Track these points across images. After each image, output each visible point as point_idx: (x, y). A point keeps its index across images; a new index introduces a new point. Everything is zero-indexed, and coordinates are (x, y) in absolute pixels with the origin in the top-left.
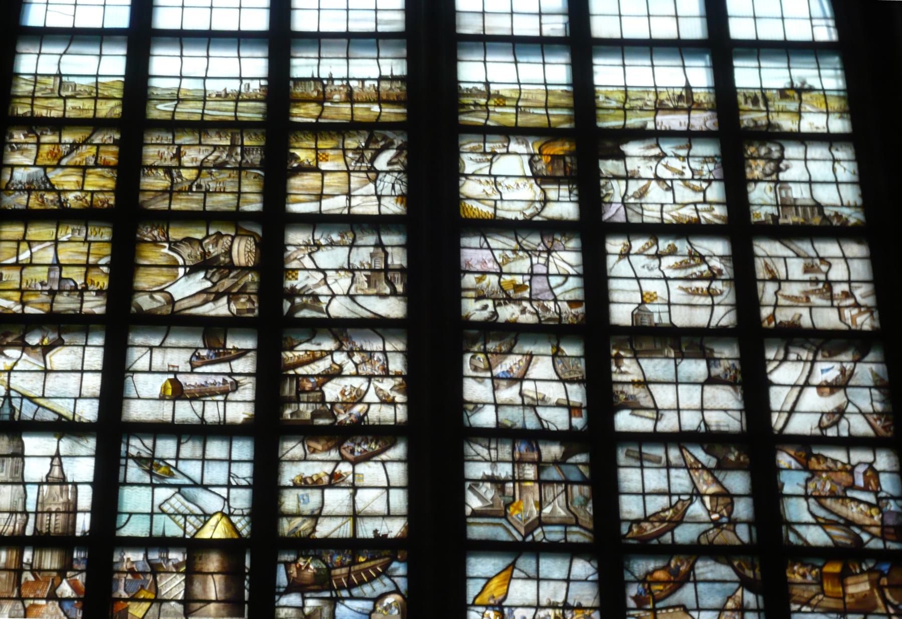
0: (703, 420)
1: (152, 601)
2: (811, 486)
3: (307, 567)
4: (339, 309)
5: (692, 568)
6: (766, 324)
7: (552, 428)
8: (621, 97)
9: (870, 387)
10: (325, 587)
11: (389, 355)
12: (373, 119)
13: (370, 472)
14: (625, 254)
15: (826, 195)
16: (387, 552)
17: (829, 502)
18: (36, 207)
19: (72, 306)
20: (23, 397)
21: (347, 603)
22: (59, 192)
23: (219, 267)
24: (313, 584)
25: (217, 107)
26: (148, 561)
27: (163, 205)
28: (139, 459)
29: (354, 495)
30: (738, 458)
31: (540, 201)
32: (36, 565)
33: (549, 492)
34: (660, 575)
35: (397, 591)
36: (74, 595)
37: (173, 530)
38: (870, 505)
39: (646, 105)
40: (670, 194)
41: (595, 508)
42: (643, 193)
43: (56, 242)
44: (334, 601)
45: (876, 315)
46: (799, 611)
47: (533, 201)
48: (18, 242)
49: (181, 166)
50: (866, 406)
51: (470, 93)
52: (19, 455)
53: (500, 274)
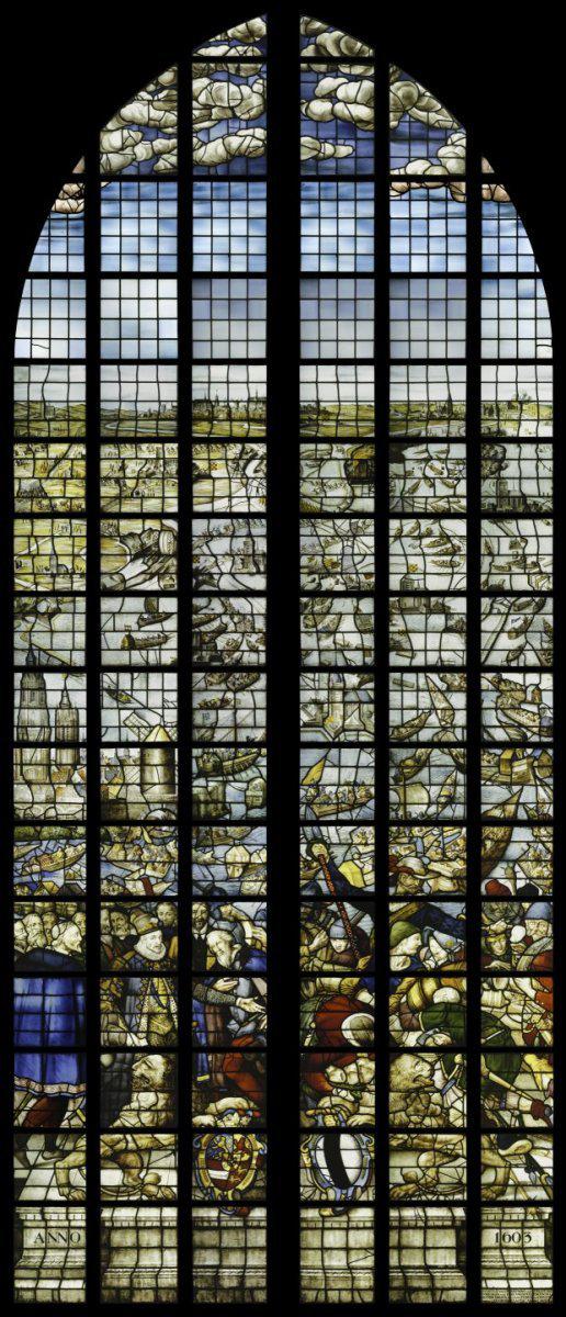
0: (440, 658)
1: (123, 785)
2: (500, 701)
4: (226, 583)
7: (353, 664)
8: (404, 409)
14: (399, 536)
15: (530, 488)
16: (255, 750)
17: (509, 712)
19: (66, 586)
20: (40, 649)
22: (51, 498)
26: (118, 758)
27: (114, 509)
28: (109, 691)
29: (235, 713)
33: (350, 708)
34: (409, 762)
35: (262, 777)
37: (133, 737)
38: (534, 714)
41: (376, 719)
43: (53, 537)
44: (225, 783)
45: (551, 579)
46: (485, 785)
47: (346, 498)
48: (29, 537)
49: (125, 477)
50: (537, 645)
51: (308, 410)
52: (43, 688)
53: (323, 556)
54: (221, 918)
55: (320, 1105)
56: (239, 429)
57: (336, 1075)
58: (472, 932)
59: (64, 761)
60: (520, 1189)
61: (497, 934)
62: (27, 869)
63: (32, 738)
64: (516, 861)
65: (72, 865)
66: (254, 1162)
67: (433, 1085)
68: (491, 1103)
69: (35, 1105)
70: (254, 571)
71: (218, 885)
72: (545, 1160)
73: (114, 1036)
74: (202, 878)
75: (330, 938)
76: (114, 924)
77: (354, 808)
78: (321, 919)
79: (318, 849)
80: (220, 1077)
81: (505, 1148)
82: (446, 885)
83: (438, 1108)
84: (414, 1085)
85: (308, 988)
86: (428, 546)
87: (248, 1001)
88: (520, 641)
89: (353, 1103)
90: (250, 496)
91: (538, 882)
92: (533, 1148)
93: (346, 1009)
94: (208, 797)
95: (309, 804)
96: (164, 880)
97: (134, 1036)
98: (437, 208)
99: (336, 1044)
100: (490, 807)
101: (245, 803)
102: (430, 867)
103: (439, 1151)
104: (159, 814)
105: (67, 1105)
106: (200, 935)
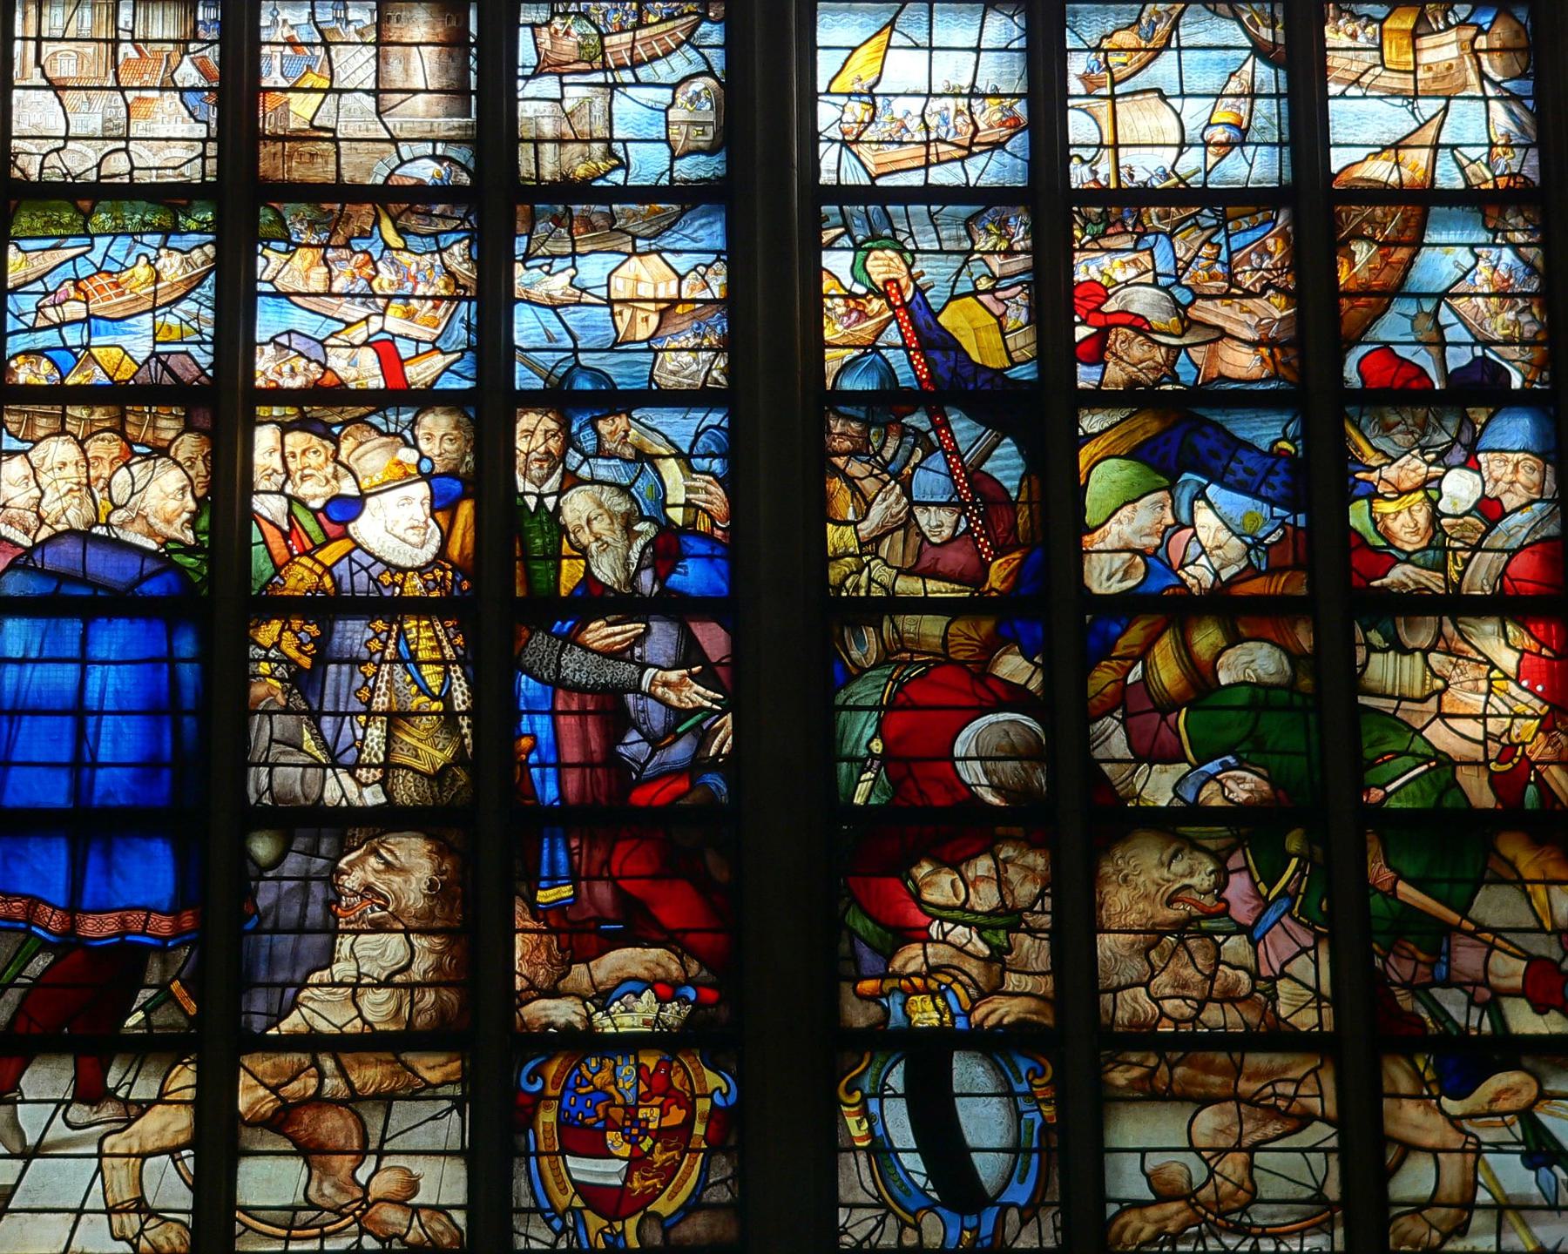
1: (326, 92)
3: (567, 33)
5: (1175, 26)
10: (596, 65)
16: (691, 7)
21: (630, 91)
24: (576, 62)
32: (139, 34)
35: (710, 73)
36: (203, 83)
46: (1343, 95)
54: (600, 452)
55: (897, 963)
57: (941, 888)
59: (156, 33)
60: (1510, 1216)
62: (50, 312)
64: (1442, 296)
66: (699, 1129)
67: (1225, 912)
68: (1407, 969)
69: (45, 971)
73: (289, 778)
75: (912, 503)
76: (293, 465)
77: (971, 154)
78: (888, 454)
79: (883, 265)
80: (603, 891)
82: (1242, 362)
83: (1241, 974)
84: (1171, 914)
85: (860, 643)
87: (673, 676)
89: (987, 961)
91: (1514, 352)
92: (1543, 1096)
93: (964, 701)
94: (566, 128)
99: (940, 799)
100: (1360, 154)
101: (667, 141)
102: (1193, 313)
103: (1252, 1101)
104: (426, 171)
105: (142, 968)
106: (540, 497)
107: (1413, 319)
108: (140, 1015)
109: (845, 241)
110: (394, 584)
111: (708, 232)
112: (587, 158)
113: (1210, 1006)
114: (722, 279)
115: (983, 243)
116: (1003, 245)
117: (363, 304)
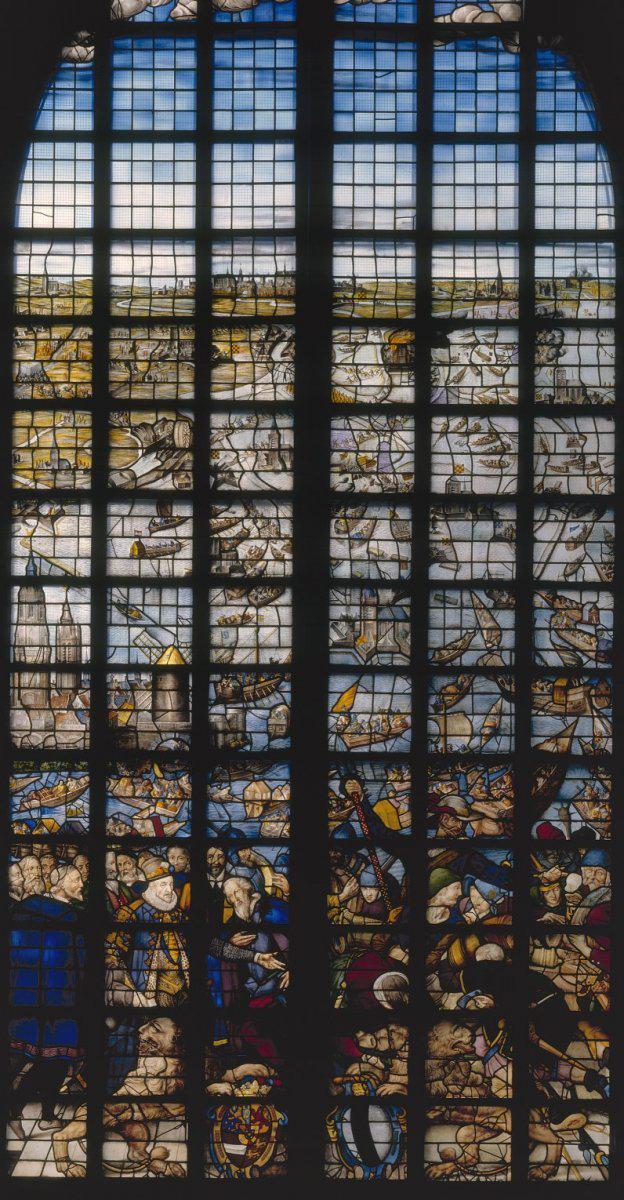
1: (132, 711)
2: (554, 620)
4: (247, 483)
5: (471, 684)
6: (536, 491)
7: (388, 578)
8: (449, 287)
9: (601, 542)
11: (281, 521)
12: (270, 313)
13: (268, 614)
14: (445, 433)
15: (590, 377)
17: (564, 634)
18: (39, 397)
19: (67, 483)
20: (42, 557)
22: (54, 384)
23: (166, 449)
25: (160, 304)
27: (124, 395)
28: (119, 606)
29: (257, 631)
30: (508, 600)
31: (387, 386)
32: (59, 685)
34: (451, 689)
35: (285, 703)
36: (84, 707)
37: (143, 659)
38: (591, 635)
39: (468, 295)
40: (479, 378)
42: (461, 376)
43: (54, 428)
44: (245, 710)
45: (613, 482)
46: (537, 715)
47: (383, 387)
48: (29, 428)
49: (136, 360)
50: (597, 558)
51: (342, 287)
52: (42, 602)
53: (357, 452)
54: (239, 864)
56: (267, 307)
57: (367, 1042)
58: (520, 885)
59: (65, 685)
60: (572, 1168)
61: (550, 882)
62: (26, 804)
63: (30, 660)
64: (571, 801)
65: (75, 800)
66: (273, 1134)
70: (280, 468)
71: (234, 825)
72: (601, 1135)
73: (120, 995)
74: (217, 817)
75: (360, 886)
76: (121, 869)
77: (388, 739)
81: (557, 1122)
82: (490, 828)
83: (479, 1076)
84: (454, 1052)
85: (339, 943)
86: (477, 444)
87: (267, 956)
88: (579, 552)
89: (383, 1070)
90: (275, 383)
92: (589, 1123)
95: (340, 734)
96: (176, 819)
97: (141, 995)
98: (487, 60)
100: (542, 740)
101: (267, 732)
102: (473, 807)
103: (480, 1125)
104: (172, 745)
107: (559, 810)
108: (66, 1087)
109: (337, 776)
110: (159, 918)
111: (283, 772)
112: (235, 739)
113: (467, 1088)
114: (288, 792)
115: (392, 776)
116: (400, 778)
117: (147, 801)
